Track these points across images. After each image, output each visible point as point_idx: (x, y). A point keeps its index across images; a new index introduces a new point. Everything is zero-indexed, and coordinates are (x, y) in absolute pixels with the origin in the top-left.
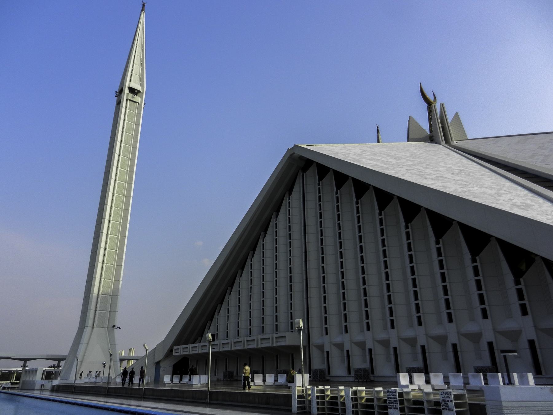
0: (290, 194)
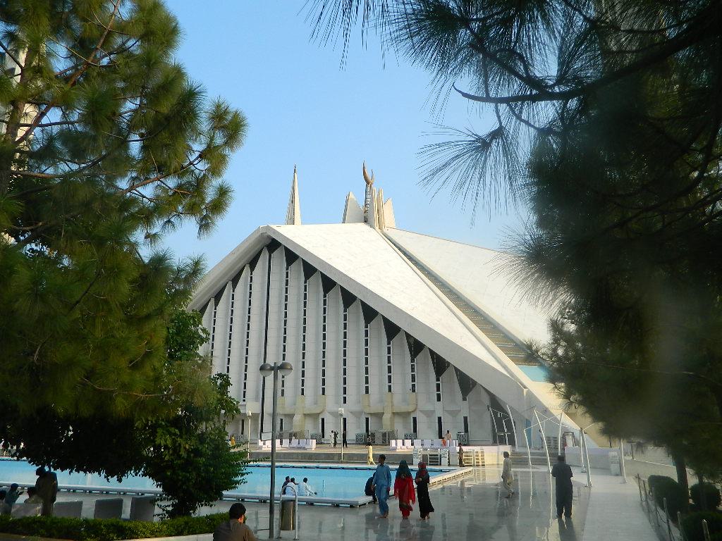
0: (252, 268)
